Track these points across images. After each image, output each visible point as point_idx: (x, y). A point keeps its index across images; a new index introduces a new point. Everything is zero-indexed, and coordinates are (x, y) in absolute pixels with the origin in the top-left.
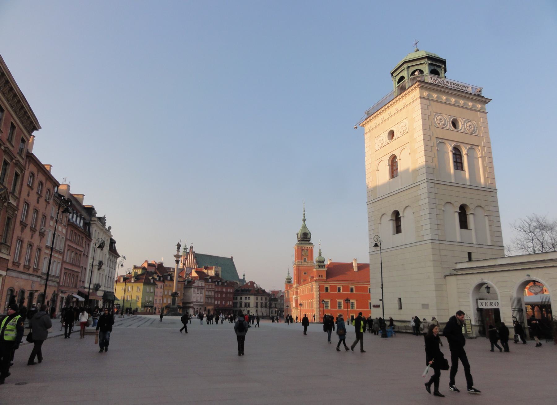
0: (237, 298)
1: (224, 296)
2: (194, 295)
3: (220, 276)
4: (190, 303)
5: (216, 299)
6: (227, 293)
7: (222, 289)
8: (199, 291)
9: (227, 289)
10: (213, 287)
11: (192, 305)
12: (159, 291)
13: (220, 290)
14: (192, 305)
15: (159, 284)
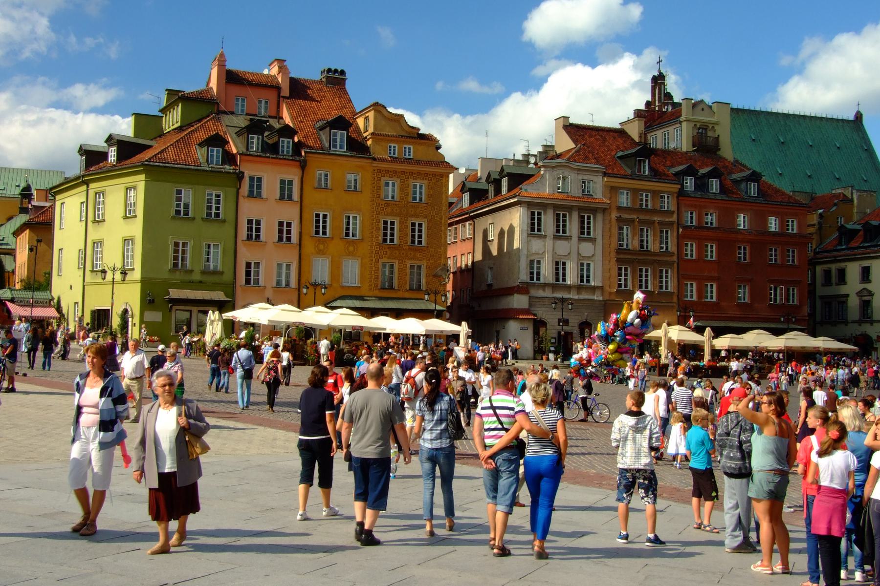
0: (842, 273)
1: (744, 254)
2: (537, 245)
3: (727, 152)
4: (510, 291)
5: (687, 271)
6: (760, 239)
7: (728, 216)
8: (573, 227)
9: (760, 219)
10: (669, 204)
11: (519, 301)
12: (269, 212)
13: (711, 219)
14: (519, 301)
15: (271, 176)
